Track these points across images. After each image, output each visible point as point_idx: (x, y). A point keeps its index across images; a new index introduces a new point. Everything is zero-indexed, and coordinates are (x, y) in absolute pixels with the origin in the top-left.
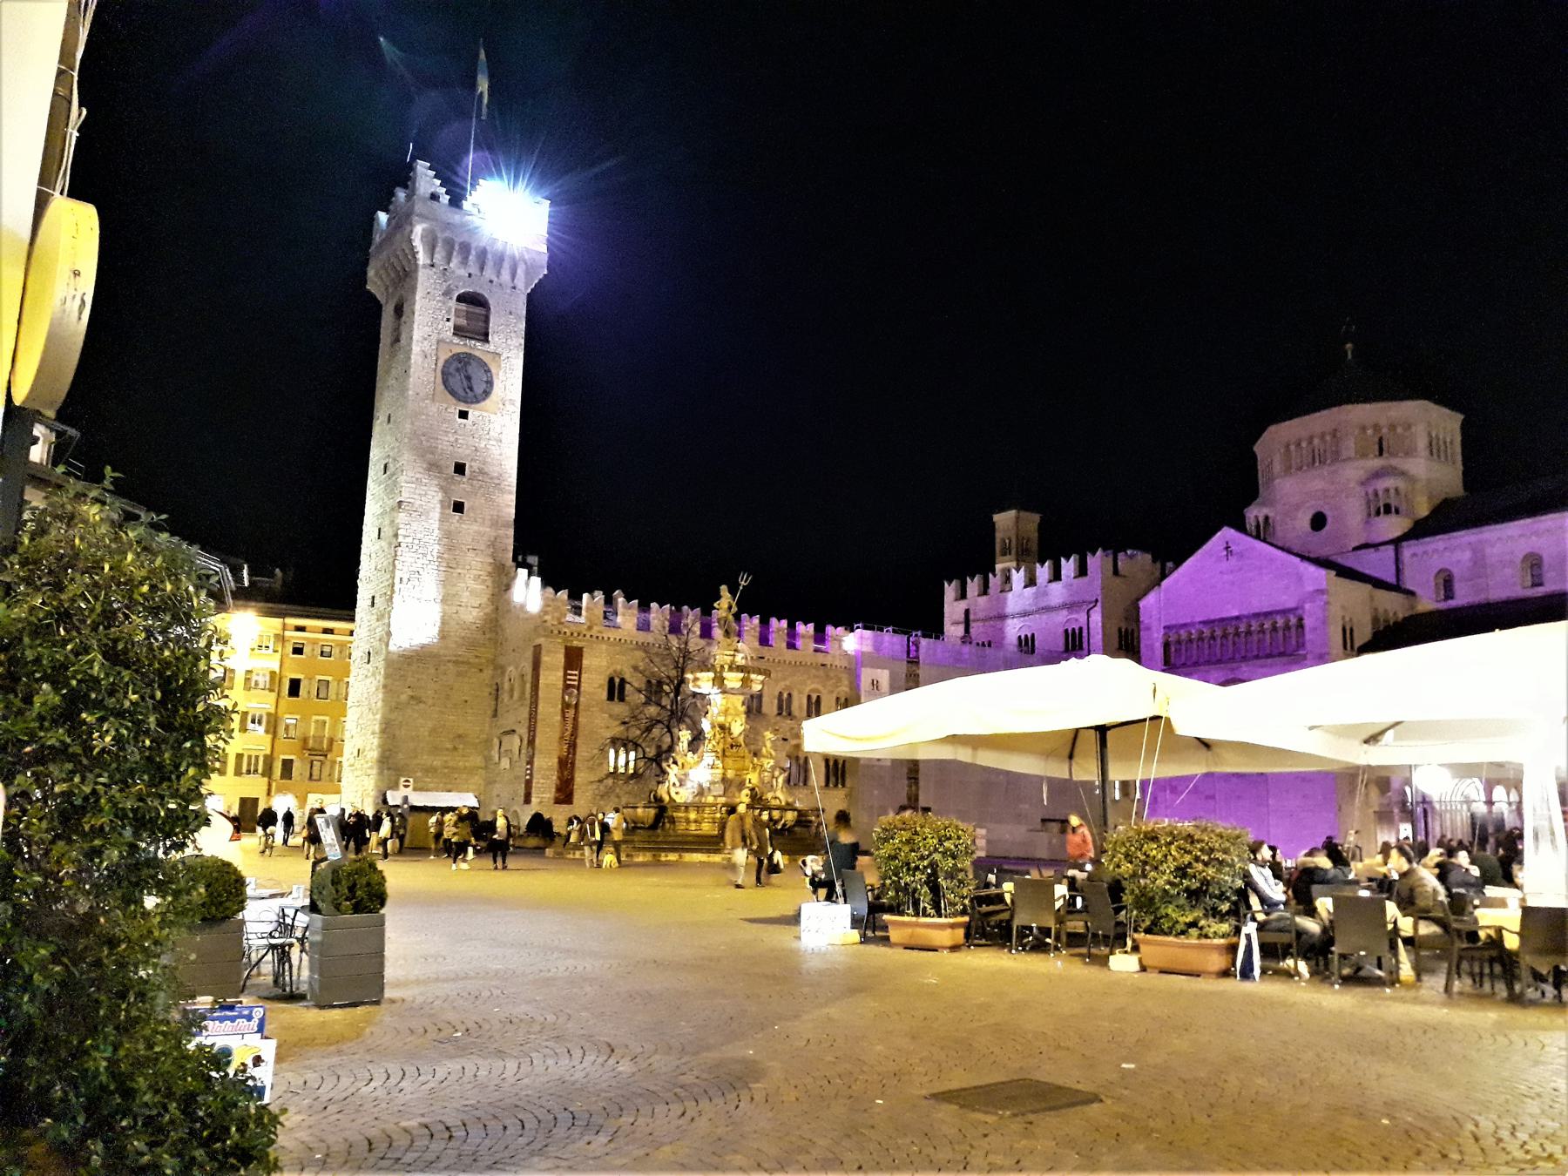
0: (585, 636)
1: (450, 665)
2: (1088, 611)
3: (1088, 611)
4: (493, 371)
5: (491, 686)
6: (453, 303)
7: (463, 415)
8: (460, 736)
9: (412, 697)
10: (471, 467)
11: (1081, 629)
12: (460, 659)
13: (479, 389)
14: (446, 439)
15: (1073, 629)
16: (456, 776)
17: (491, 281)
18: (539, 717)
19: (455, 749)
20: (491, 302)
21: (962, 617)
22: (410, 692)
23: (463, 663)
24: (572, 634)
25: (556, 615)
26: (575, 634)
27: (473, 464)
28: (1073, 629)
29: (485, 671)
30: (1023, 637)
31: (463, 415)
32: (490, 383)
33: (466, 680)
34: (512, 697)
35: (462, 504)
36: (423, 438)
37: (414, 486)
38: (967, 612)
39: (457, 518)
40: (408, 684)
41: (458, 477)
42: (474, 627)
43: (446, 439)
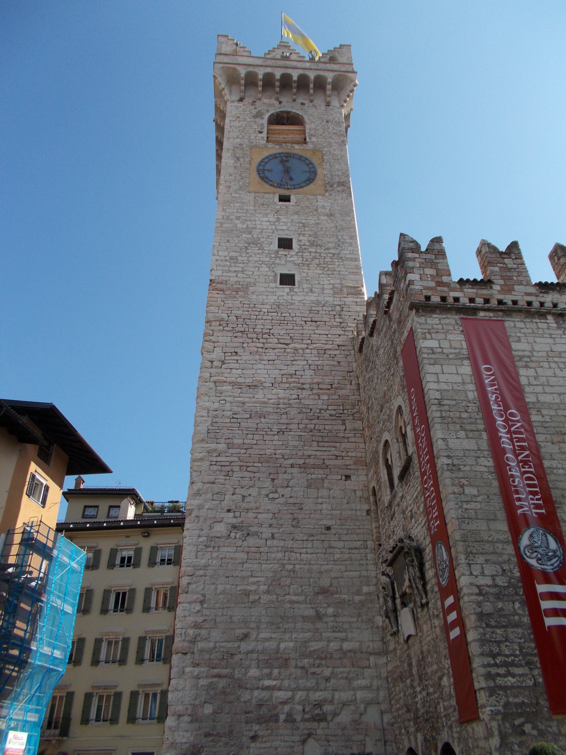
1: (295, 470)
4: (315, 160)
7: (284, 199)
8: (324, 591)
9: (234, 527)
10: (300, 241)
12: (311, 461)
16: (327, 672)
17: (303, 104)
18: (442, 462)
19: (319, 617)
20: (306, 118)
22: (229, 518)
23: (314, 467)
24: (472, 300)
27: (301, 238)
29: (353, 478)
33: (324, 492)
37: (229, 264)
39: (288, 290)
40: (226, 504)
41: (282, 252)
42: (326, 415)
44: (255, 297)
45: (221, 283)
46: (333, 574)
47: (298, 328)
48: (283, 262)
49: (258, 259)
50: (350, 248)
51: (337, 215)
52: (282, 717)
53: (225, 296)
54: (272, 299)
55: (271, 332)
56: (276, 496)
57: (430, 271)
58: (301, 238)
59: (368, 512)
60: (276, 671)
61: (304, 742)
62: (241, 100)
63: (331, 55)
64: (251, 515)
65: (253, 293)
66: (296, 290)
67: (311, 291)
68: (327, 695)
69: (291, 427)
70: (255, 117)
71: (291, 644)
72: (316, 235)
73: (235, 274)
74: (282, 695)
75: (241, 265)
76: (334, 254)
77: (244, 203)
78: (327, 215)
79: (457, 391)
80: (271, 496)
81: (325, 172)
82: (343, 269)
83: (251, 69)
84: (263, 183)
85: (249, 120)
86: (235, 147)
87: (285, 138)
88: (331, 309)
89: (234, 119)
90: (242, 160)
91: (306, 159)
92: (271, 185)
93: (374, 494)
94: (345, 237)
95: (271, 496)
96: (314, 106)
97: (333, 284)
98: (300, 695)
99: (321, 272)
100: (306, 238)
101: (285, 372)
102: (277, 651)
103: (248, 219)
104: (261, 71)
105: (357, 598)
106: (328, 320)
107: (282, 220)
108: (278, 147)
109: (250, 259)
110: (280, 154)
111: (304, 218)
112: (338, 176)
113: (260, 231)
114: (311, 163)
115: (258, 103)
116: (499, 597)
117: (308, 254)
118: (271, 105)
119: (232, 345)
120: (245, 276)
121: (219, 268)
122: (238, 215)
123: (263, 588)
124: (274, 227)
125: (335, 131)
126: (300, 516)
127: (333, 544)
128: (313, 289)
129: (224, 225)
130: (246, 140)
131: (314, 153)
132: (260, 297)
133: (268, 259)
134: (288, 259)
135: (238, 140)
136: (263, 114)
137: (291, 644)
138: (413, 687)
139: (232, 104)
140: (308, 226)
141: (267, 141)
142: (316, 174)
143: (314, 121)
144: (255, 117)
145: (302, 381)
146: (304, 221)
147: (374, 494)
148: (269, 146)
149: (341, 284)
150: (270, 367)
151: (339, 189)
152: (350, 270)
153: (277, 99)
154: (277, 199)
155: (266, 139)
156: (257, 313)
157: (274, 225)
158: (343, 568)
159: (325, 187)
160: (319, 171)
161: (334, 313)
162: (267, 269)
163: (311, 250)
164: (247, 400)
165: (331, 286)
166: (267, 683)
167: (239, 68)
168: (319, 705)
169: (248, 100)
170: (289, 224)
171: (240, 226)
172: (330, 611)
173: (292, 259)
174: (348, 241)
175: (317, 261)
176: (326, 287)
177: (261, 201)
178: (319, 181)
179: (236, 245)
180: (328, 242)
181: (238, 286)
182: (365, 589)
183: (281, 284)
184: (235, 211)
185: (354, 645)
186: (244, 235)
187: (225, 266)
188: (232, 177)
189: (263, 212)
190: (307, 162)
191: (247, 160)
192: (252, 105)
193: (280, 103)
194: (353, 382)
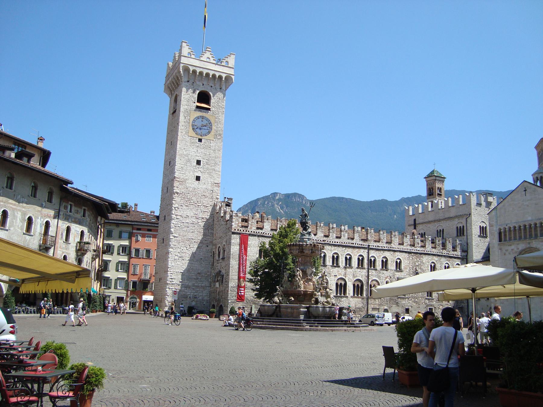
0: (249, 231)
2: (466, 219)
3: (466, 219)
4: (212, 121)
5: (211, 253)
7: (200, 140)
8: (199, 273)
10: (203, 162)
11: (463, 226)
14: (193, 150)
15: (460, 227)
16: (198, 290)
17: (212, 87)
19: (197, 279)
21: (413, 223)
24: (243, 231)
25: (237, 222)
26: (245, 231)
27: (204, 160)
28: (460, 227)
30: (439, 230)
31: (200, 140)
33: (201, 250)
34: (219, 257)
35: (200, 177)
36: (184, 151)
38: (415, 220)
41: (198, 166)
43: (193, 150)
46: (201, 270)
48: (197, 171)
50: (219, 167)
51: (217, 151)
52: (188, 297)
54: (193, 186)
56: (190, 250)
57: (237, 222)
59: (211, 256)
60: (188, 289)
61: (192, 302)
62: (188, 81)
64: (184, 254)
68: (198, 294)
69: (195, 231)
71: (191, 284)
74: (189, 293)
75: (185, 171)
78: (213, 150)
79: (235, 252)
80: (189, 250)
83: (194, 68)
91: (209, 121)
93: (214, 254)
94: (218, 161)
95: (189, 250)
96: (216, 88)
98: (192, 293)
101: (195, 213)
102: (188, 285)
105: (206, 275)
109: (187, 168)
114: (211, 123)
116: (234, 288)
118: (199, 86)
119: (181, 202)
122: (185, 147)
123: (186, 272)
126: (195, 255)
127: (202, 263)
129: (180, 152)
137: (191, 284)
138: (216, 295)
139: (185, 84)
145: (199, 216)
146: (205, 153)
147: (214, 254)
150: (191, 211)
151: (219, 137)
152: (217, 176)
154: (197, 141)
158: (203, 268)
160: (214, 128)
164: (184, 222)
166: (186, 291)
167: (190, 67)
168: (196, 296)
169: (191, 82)
171: (185, 153)
172: (200, 278)
173: (200, 170)
174: (218, 163)
175: (207, 171)
176: (209, 182)
178: (213, 133)
182: (208, 273)
185: (204, 285)
187: (179, 170)
190: (210, 122)
192: (193, 85)
193: (203, 85)
194: (213, 218)
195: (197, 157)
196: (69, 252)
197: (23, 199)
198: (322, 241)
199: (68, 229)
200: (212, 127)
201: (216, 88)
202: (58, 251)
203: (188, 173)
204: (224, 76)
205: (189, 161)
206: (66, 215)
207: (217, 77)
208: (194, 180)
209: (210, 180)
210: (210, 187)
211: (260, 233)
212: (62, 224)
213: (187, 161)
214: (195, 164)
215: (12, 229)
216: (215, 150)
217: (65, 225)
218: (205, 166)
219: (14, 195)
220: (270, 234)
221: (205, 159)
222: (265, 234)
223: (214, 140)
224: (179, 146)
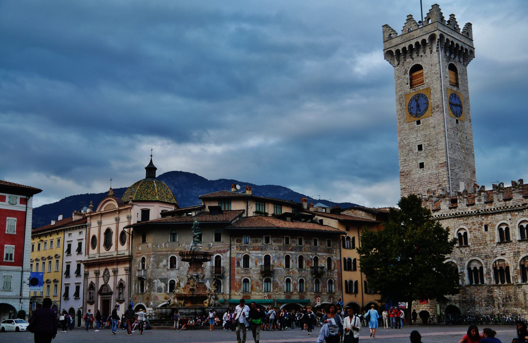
4: (427, 96)
6: (408, 76)
7: (418, 123)
10: (425, 145)
13: (422, 108)
14: (413, 136)
17: (422, 56)
20: (423, 66)
27: (425, 143)
31: (418, 123)
32: (427, 103)
36: (404, 141)
37: (403, 163)
39: (422, 170)
44: (412, 176)
45: (403, 172)
47: (425, 187)
48: (420, 157)
49: (412, 158)
50: (441, 144)
51: (437, 126)
53: (404, 178)
54: (418, 176)
55: (418, 190)
58: (425, 143)
62: (398, 64)
63: (428, 18)
65: (412, 174)
66: (424, 170)
67: (429, 169)
70: (405, 74)
72: (429, 140)
73: (406, 167)
75: (408, 162)
76: (436, 148)
77: (406, 130)
81: (432, 101)
82: (439, 155)
83: (397, 48)
84: (411, 116)
85: (403, 77)
86: (400, 98)
87: (418, 81)
88: (435, 176)
89: (397, 79)
90: (403, 104)
91: (425, 95)
92: (414, 117)
94: (439, 138)
97: (436, 164)
99: (432, 159)
100: (426, 143)
103: (407, 138)
104: (400, 48)
106: (434, 181)
107: (419, 135)
108: (414, 91)
109: (410, 158)
110: (415, 96)
111: (425, 132)
112: (436, 102)
113: (411, 143)
114: (426, 98)
115: (404, 64)
117: (427, 151)
118: (410, 63)
120: (409, 167)
121: (402, 165)
122: (405, 137)
124: (416, 140)
125: (434, 71)
128: (430, 168)
130: (403, 91)
131: (427, 90)
132: (414, 176)
133: (415, 157)
134: (422, 155)
135: (400, 93)
136: (407, 71)
140: (427, 136)
141: (411, 88)
142: (428, 104)
143: (426, 67)
144: (405, 74)
146: (425, 134)
148: (411, 92)
149: (438, 163)
151: (437, 110)
152: (441, 155)
153: (411, 58)
155: (409, 88)
156: (414, 183)
157: (416, 139)
159: (432, 110)
161: (436, 177)
162: (415, 162)
163: (429, 148)
165: (435, 165)
169: (401, 63)
170: (421, 137)
171: (406, 143)
173: (423, 155)
174: (440, 140)
175: (430, 153)
177: (411, 126)
178: (429, 109)
179: (405, 153)
180: (434, 143)
181: (408, 173)
183: (420, 168)
184: (403, 135)
186: (408, 147)
188: (400, 116)
189: (413, 132)
190: (425, 97)
191: (404, 103)
192: (403, 65)
195: (418, 142)
196: (251, 275)
197: (188, 245)
198: (521, 205)
199: (246, 258)
200: (428, 102)
201: (426, 55)
202: (236, 277)
203: (411, 163)
204: (426, 37)
205: (411, 150)
206: (240, 247)
207: (420, 43)
208: (417, 169)
209: (435, 163)
210: (435, 171)
211: (437, 216)
212: (237, 254)
213: (409, 151)
214: (417, 150)
215: (181, 268)
216: (435, 127)
217: (240, 255)
218: (427, 148)
219: (179, 245)
220: (448, 215)
221: (426, 141)
222: (443, 216)
223: (433, 115)
224: (400, 138)
